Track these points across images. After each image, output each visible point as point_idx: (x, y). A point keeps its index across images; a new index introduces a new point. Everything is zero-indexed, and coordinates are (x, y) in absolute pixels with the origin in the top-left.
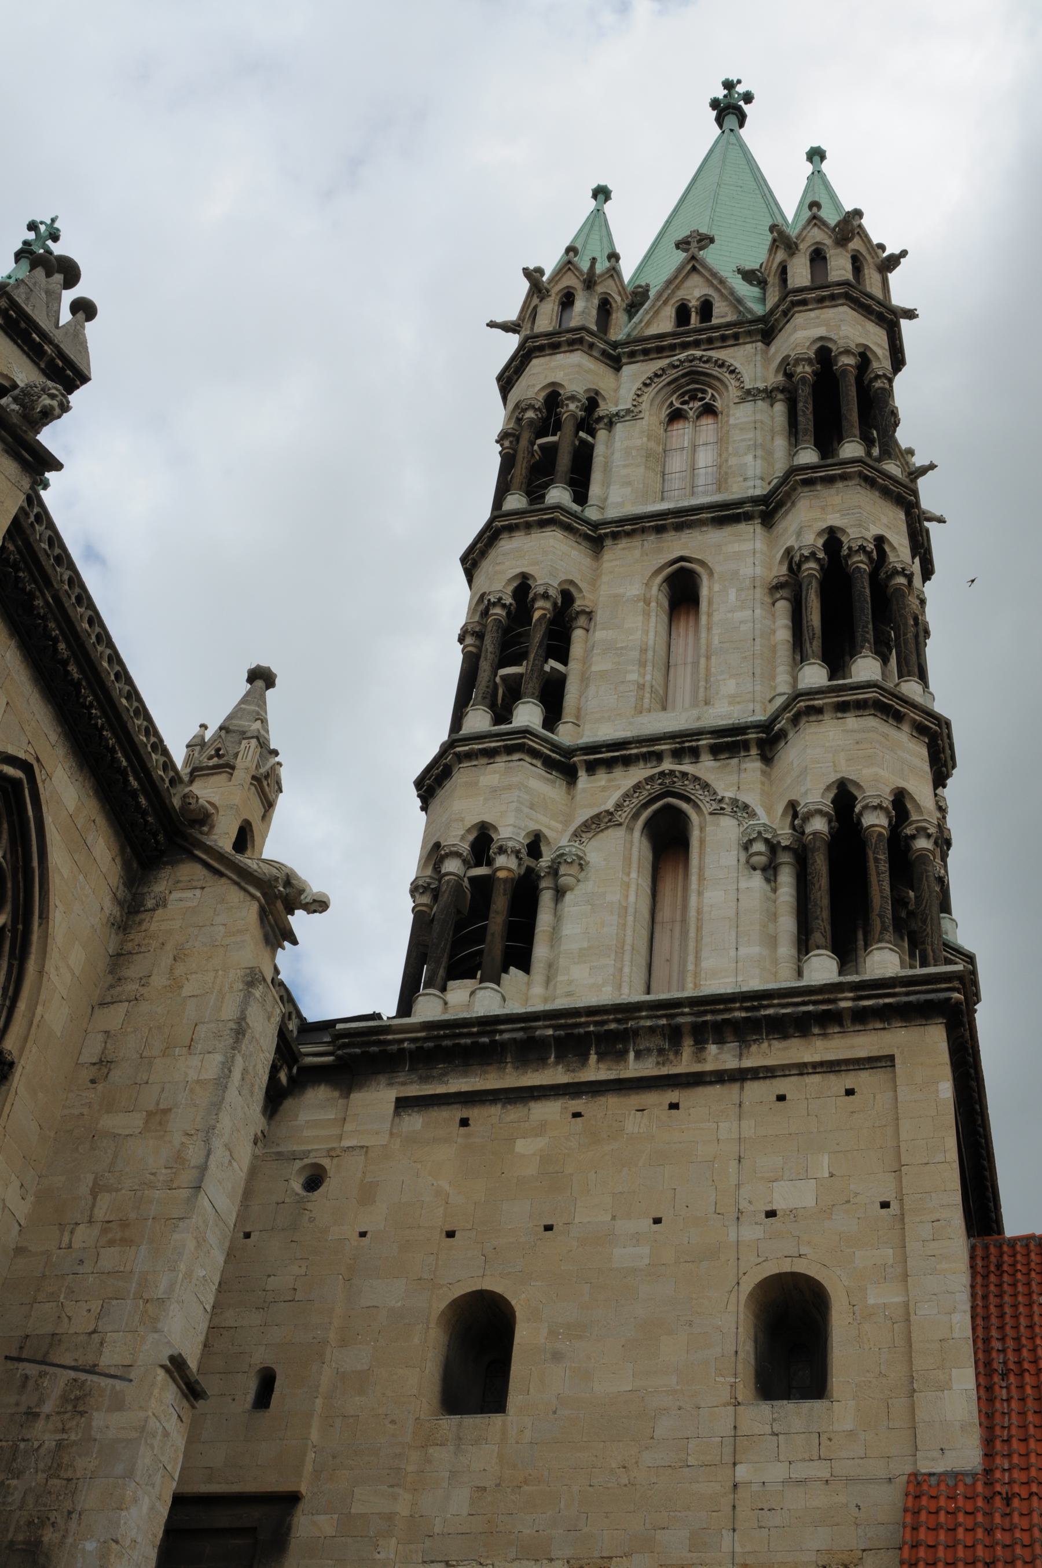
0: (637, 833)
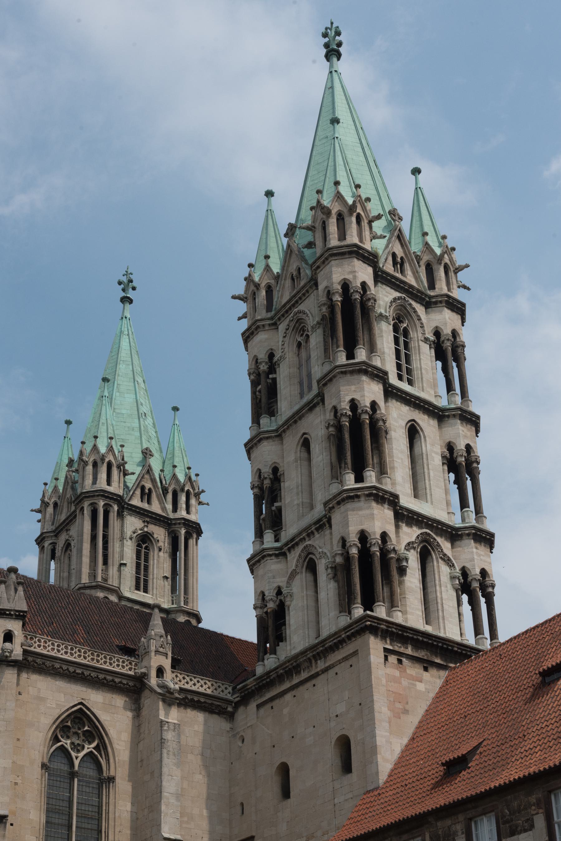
0: (304, 574)
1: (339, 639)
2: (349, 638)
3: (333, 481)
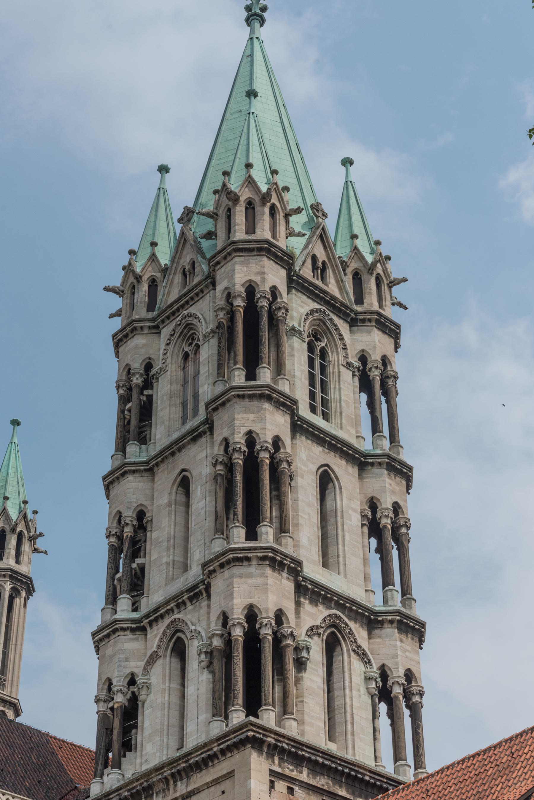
0: (168, 659)
1: (209, 753)
2: (223, 752)
3: (217, 536)
